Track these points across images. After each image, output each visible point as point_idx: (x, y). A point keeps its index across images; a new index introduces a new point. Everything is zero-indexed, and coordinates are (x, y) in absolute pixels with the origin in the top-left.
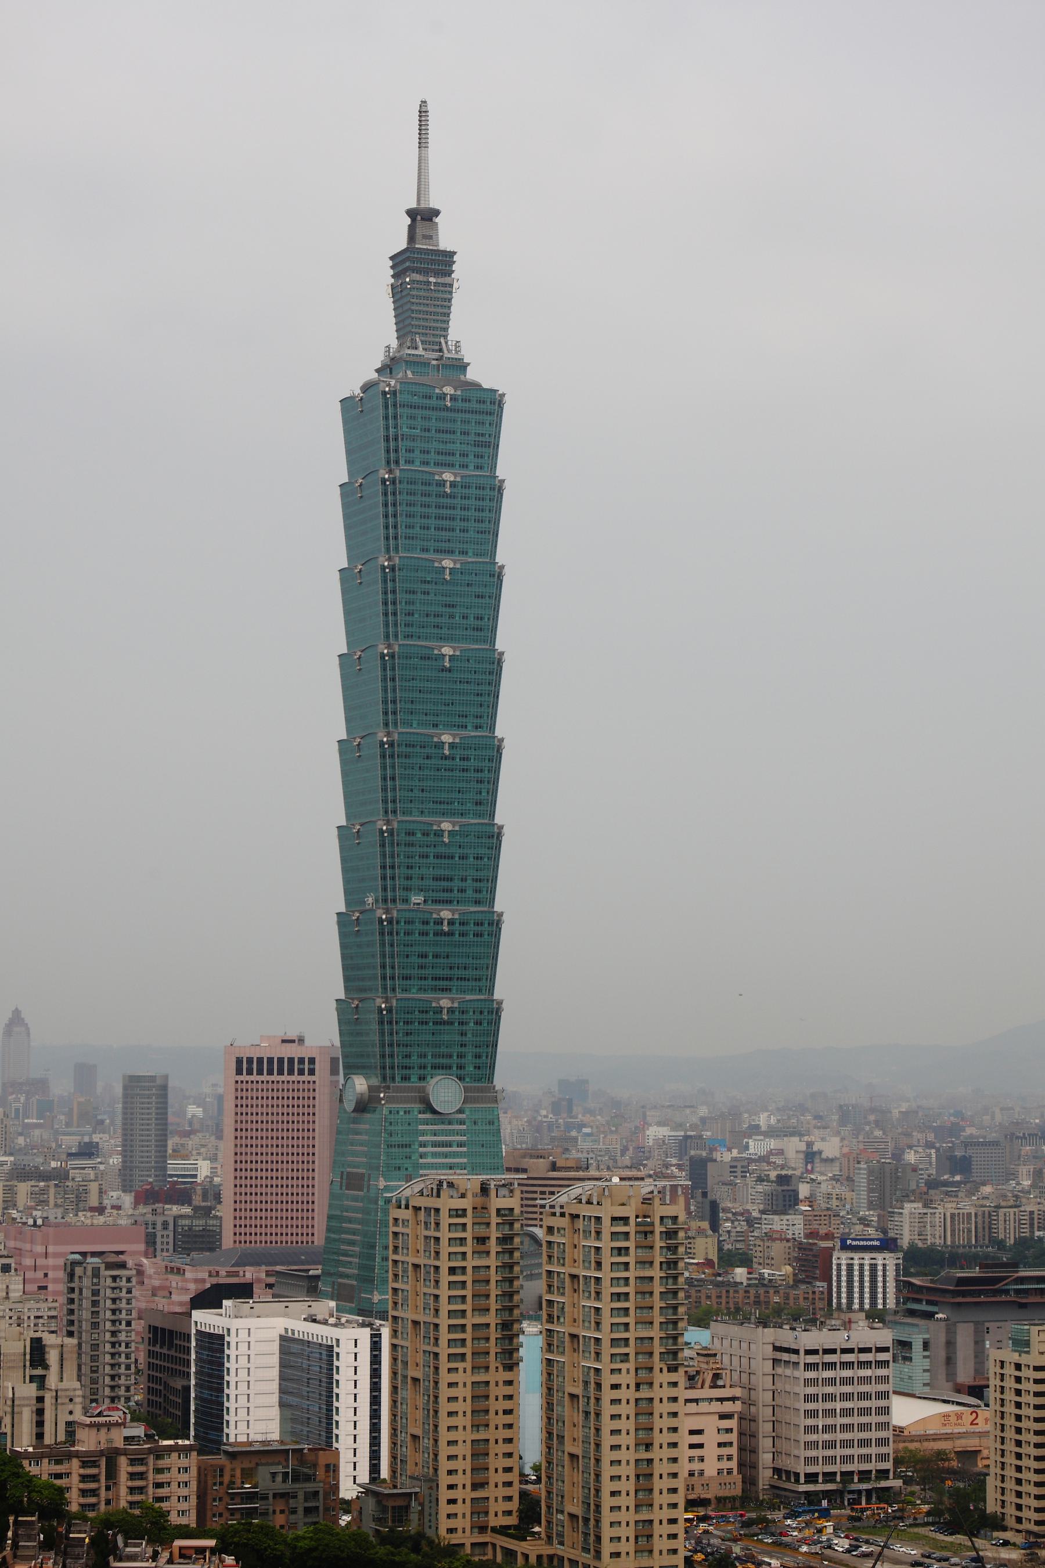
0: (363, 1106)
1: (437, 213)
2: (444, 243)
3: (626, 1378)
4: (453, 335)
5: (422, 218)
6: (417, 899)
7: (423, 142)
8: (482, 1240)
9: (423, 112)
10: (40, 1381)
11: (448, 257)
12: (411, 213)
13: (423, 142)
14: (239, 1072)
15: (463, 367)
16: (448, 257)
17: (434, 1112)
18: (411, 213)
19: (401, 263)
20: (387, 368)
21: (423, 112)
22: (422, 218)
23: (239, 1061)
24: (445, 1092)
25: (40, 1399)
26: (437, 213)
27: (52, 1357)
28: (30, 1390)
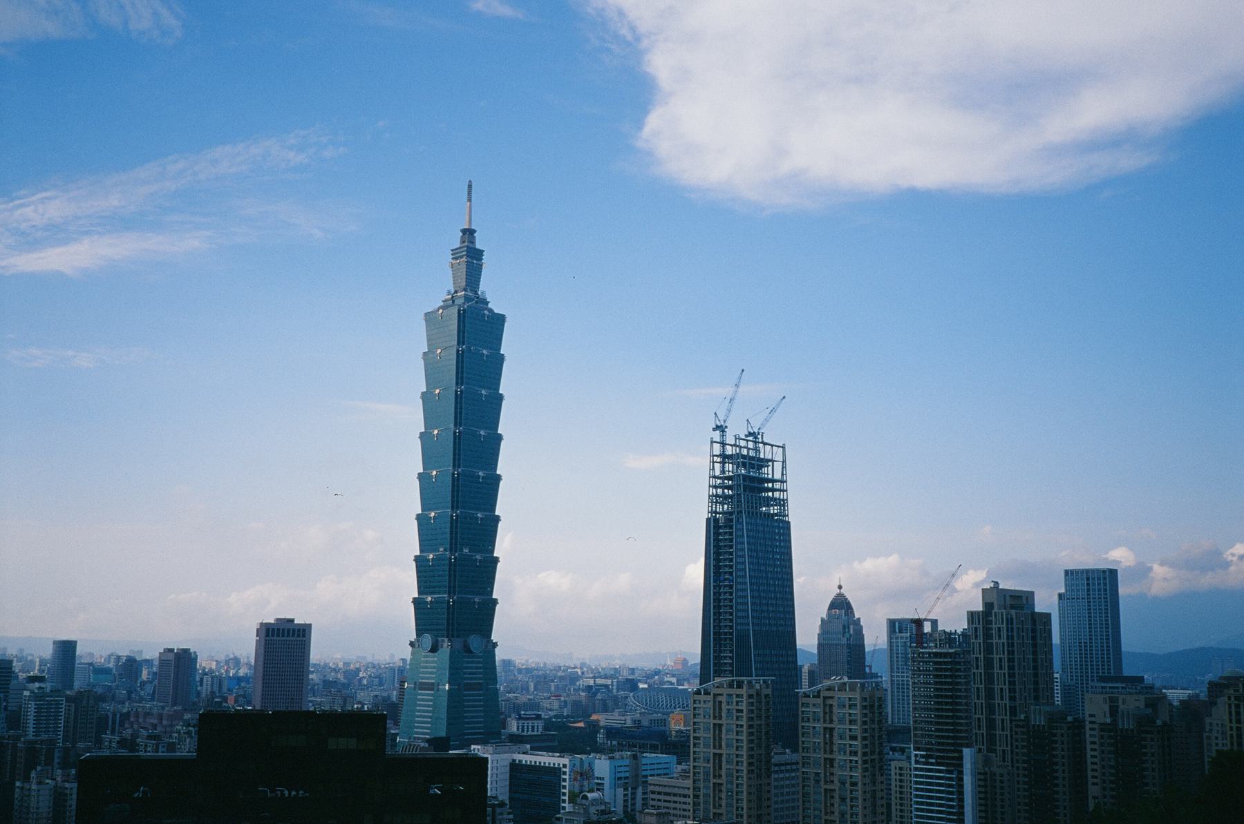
1: (475, 231)
2: (478, 246)
3: (867, 781)
4: (481, 288)
5: (469, 233)
6: (466, 550)
7: (470, 200)
9: (470, 186)
11: (480, 253)
12: (464, 231)
13: (470, 200)
14: (267, 635)
16: (480, 253)
17: (470, 652)
18: (464, 231)
19: (455, 252)
21: (470, 186)
22: (469, 233)
23: (268, 630)
24: (475, 642)
26: (475, 231)
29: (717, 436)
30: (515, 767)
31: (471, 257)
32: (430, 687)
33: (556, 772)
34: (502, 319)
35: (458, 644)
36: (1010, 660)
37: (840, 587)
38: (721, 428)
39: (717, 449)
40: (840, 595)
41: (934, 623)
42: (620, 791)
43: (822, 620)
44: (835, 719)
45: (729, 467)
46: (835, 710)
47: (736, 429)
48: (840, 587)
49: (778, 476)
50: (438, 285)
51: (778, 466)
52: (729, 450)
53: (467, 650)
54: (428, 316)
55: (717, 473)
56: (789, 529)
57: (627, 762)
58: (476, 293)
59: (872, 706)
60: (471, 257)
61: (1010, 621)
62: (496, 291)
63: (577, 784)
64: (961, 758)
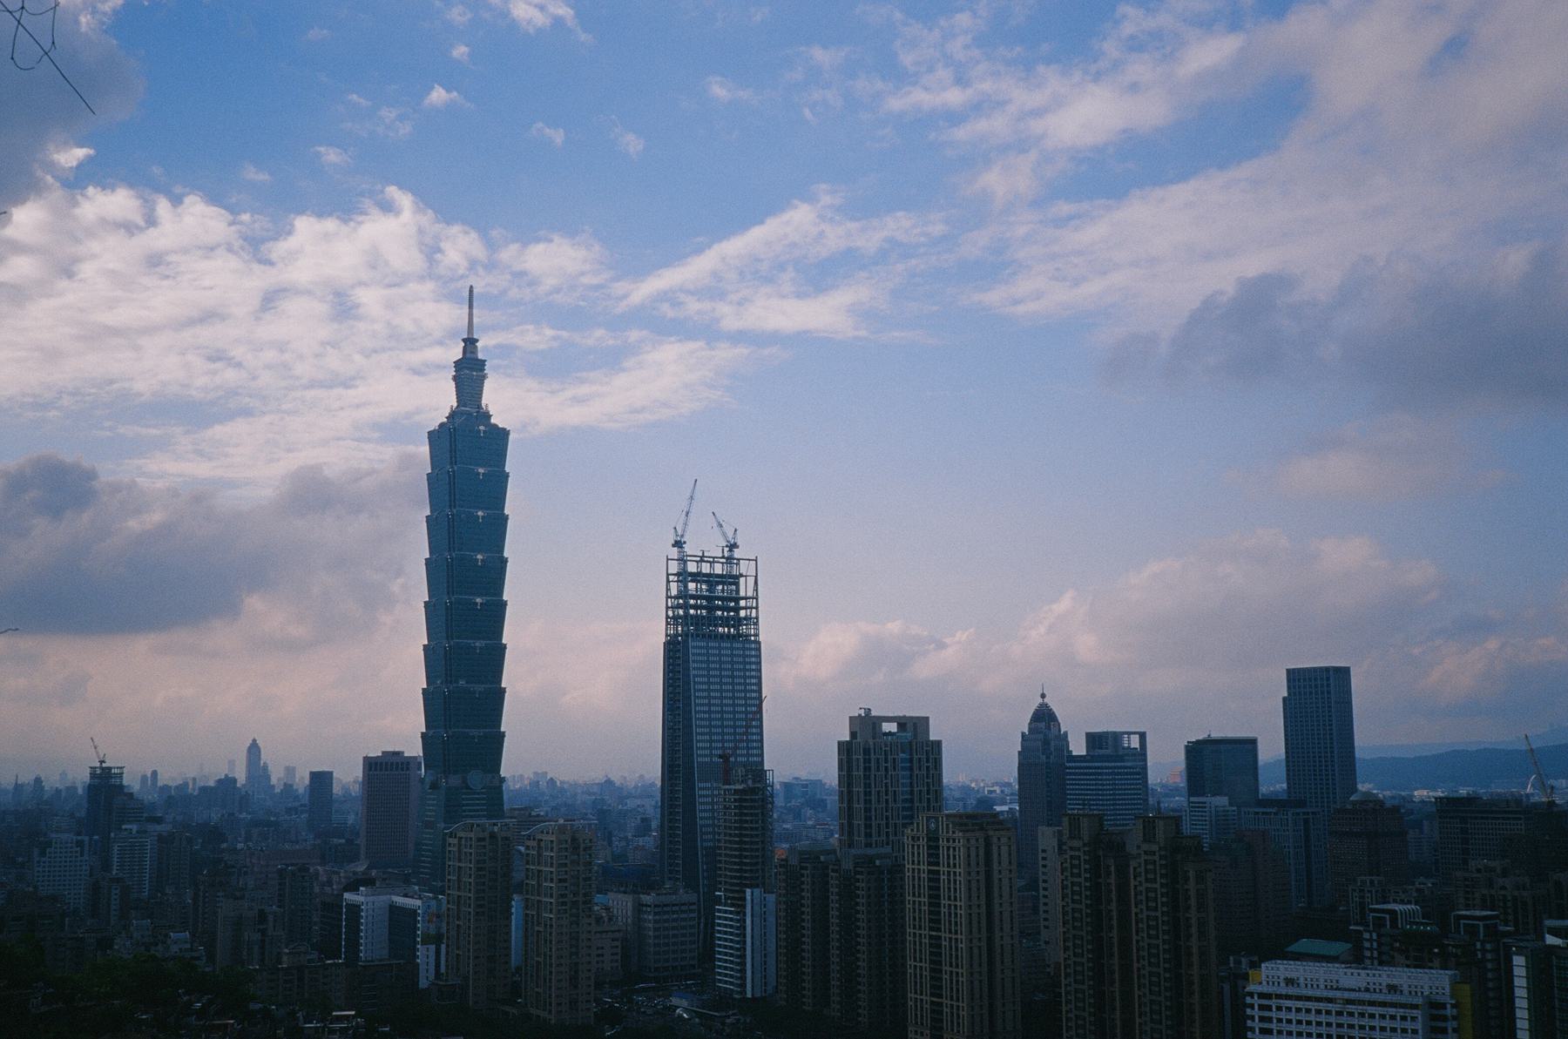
2: (480, 356)
4: (484, 402)
10: (263, 932)
11: (481, 365)
13: (471, 307)
15: (488, 416)
20: (453, 415)
24: (476, 779)
25: (263, 941)
27: (271, 918)
28: (258, 936)
29: (674, 553)
30: (393, 908)
31: (469, 373)
33: (413, 913)
34: (503, 434)
35: (455, 780)
37: (1043, 696)
38: (678, 544)
39: (674, 567)
40: (1041, 705)
41: (1142, 736)
43: (1023, 735)
45: (692, 586)
47: (705, 543)
48: (1043, 696)
49: (750, 594)
51: (751, 581)
52: (692, 567)
55: (674, 592)
56: (759, 649)
58: (479, 406)
59: (576, 849)
61: (867, 751)
62: (502, 401)
63: (432, 926)
64: (744, 899)
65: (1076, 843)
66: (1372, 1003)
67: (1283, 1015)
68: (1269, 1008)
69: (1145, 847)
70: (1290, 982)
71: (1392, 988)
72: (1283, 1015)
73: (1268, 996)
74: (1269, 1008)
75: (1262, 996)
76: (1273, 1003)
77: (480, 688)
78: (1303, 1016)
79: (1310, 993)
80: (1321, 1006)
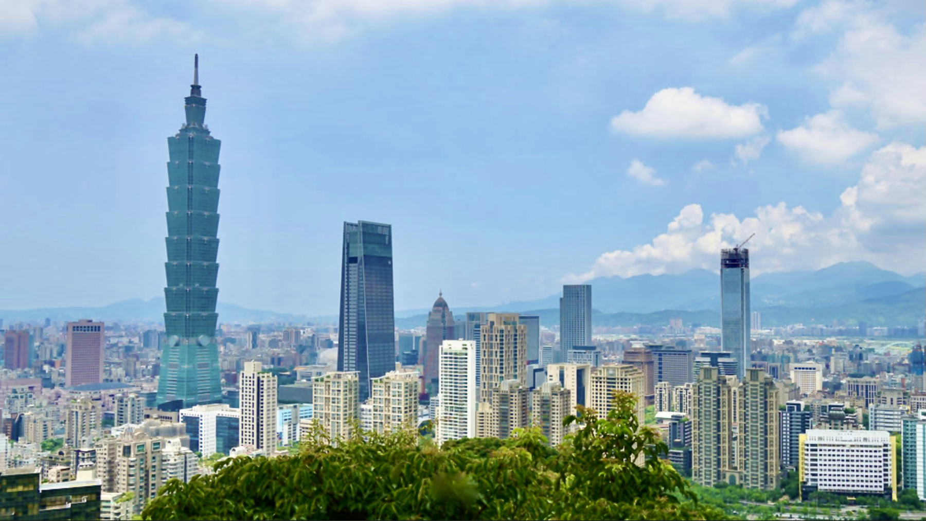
0: (177, 345)
6: (197, 285)
8: (350, 390)
24: (203, 339)
31: (196, 103)
32: (175, 366)
35: (193, 341)
36: (501, 352)
42: (286, 427)
44: (391, 393)
46: (391, 389)
50: (176, 120)
53: (200, 345)
54: (170, 139)
57: (290, 410)
60: (196, 103)
65: (708, 381)
66: (862, 446)
67: (822, 453)
68: (816, 450)
69: (751, 383)
70: (820, 439)
71: (865, 439)
72: (822, 453)
73: (816, 445)
74: (816, 450)
75: (812, 445)
76: (818, 448)
77: (205, 289)
78: (831, 453)
79: (832, 443)
80: (840, 448)
